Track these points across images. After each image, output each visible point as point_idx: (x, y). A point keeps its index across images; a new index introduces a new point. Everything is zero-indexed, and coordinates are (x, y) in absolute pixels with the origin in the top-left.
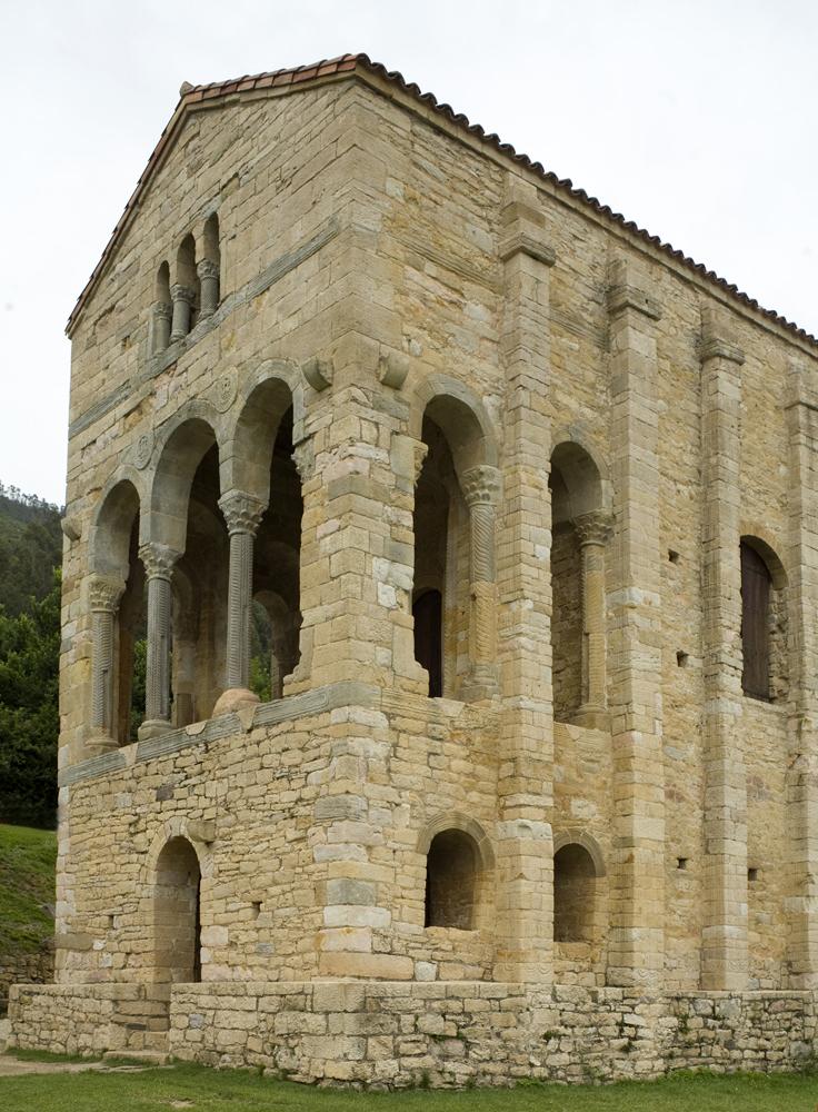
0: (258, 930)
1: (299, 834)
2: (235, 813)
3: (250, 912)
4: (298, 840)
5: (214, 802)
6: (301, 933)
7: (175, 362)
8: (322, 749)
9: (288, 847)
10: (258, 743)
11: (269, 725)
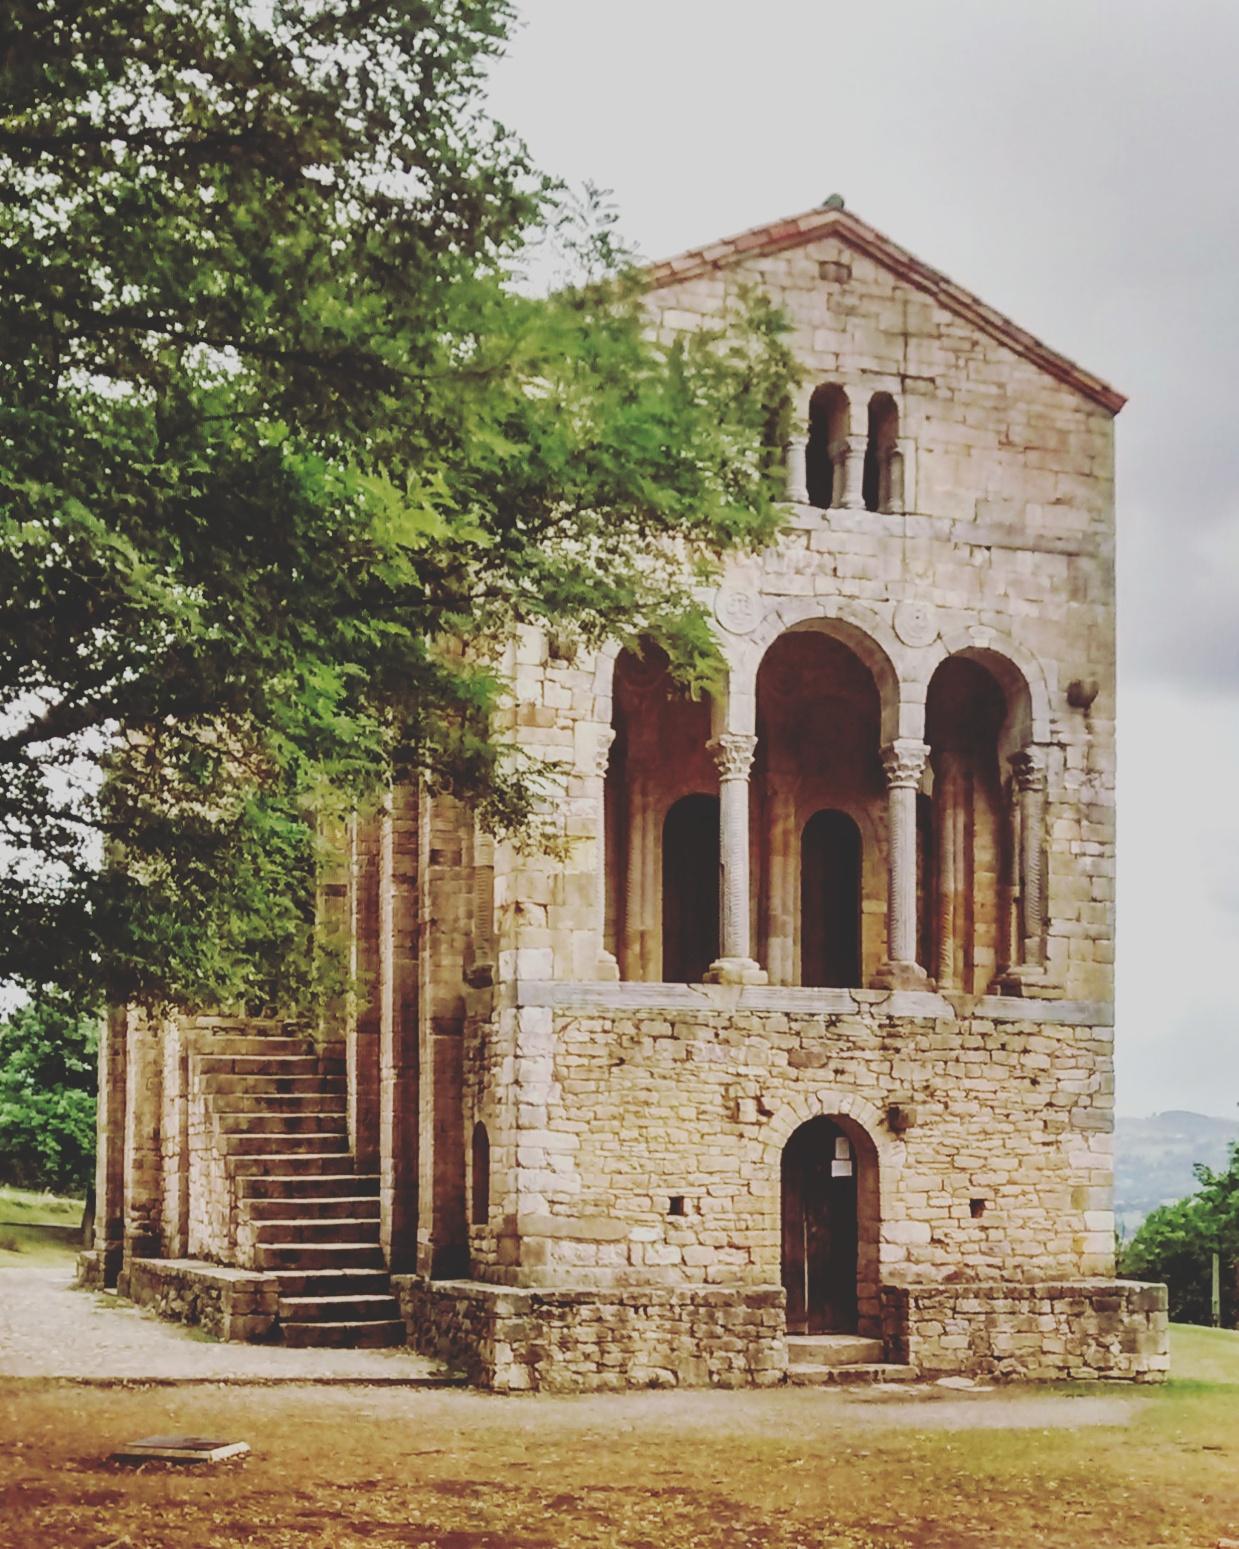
0: (984, 1229)
1: (1052, 1138)
2: (946, 1106)
3: (968, 1210)
4: (1044, 1144)
5: (906, 1085)
6: (1052, 1235)
7: (808, 532)
8: (1081, 1062)
9: (1033, 1149)
10: (983, 1035)
11: (997, 1022)
